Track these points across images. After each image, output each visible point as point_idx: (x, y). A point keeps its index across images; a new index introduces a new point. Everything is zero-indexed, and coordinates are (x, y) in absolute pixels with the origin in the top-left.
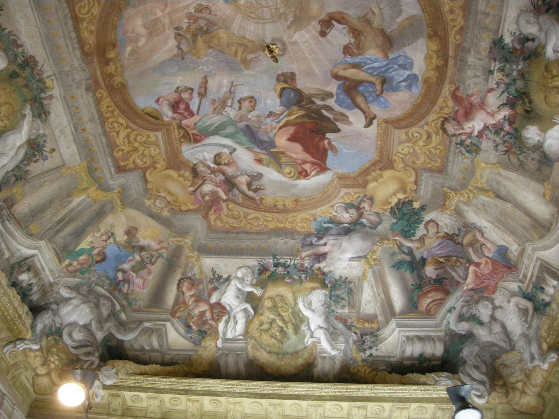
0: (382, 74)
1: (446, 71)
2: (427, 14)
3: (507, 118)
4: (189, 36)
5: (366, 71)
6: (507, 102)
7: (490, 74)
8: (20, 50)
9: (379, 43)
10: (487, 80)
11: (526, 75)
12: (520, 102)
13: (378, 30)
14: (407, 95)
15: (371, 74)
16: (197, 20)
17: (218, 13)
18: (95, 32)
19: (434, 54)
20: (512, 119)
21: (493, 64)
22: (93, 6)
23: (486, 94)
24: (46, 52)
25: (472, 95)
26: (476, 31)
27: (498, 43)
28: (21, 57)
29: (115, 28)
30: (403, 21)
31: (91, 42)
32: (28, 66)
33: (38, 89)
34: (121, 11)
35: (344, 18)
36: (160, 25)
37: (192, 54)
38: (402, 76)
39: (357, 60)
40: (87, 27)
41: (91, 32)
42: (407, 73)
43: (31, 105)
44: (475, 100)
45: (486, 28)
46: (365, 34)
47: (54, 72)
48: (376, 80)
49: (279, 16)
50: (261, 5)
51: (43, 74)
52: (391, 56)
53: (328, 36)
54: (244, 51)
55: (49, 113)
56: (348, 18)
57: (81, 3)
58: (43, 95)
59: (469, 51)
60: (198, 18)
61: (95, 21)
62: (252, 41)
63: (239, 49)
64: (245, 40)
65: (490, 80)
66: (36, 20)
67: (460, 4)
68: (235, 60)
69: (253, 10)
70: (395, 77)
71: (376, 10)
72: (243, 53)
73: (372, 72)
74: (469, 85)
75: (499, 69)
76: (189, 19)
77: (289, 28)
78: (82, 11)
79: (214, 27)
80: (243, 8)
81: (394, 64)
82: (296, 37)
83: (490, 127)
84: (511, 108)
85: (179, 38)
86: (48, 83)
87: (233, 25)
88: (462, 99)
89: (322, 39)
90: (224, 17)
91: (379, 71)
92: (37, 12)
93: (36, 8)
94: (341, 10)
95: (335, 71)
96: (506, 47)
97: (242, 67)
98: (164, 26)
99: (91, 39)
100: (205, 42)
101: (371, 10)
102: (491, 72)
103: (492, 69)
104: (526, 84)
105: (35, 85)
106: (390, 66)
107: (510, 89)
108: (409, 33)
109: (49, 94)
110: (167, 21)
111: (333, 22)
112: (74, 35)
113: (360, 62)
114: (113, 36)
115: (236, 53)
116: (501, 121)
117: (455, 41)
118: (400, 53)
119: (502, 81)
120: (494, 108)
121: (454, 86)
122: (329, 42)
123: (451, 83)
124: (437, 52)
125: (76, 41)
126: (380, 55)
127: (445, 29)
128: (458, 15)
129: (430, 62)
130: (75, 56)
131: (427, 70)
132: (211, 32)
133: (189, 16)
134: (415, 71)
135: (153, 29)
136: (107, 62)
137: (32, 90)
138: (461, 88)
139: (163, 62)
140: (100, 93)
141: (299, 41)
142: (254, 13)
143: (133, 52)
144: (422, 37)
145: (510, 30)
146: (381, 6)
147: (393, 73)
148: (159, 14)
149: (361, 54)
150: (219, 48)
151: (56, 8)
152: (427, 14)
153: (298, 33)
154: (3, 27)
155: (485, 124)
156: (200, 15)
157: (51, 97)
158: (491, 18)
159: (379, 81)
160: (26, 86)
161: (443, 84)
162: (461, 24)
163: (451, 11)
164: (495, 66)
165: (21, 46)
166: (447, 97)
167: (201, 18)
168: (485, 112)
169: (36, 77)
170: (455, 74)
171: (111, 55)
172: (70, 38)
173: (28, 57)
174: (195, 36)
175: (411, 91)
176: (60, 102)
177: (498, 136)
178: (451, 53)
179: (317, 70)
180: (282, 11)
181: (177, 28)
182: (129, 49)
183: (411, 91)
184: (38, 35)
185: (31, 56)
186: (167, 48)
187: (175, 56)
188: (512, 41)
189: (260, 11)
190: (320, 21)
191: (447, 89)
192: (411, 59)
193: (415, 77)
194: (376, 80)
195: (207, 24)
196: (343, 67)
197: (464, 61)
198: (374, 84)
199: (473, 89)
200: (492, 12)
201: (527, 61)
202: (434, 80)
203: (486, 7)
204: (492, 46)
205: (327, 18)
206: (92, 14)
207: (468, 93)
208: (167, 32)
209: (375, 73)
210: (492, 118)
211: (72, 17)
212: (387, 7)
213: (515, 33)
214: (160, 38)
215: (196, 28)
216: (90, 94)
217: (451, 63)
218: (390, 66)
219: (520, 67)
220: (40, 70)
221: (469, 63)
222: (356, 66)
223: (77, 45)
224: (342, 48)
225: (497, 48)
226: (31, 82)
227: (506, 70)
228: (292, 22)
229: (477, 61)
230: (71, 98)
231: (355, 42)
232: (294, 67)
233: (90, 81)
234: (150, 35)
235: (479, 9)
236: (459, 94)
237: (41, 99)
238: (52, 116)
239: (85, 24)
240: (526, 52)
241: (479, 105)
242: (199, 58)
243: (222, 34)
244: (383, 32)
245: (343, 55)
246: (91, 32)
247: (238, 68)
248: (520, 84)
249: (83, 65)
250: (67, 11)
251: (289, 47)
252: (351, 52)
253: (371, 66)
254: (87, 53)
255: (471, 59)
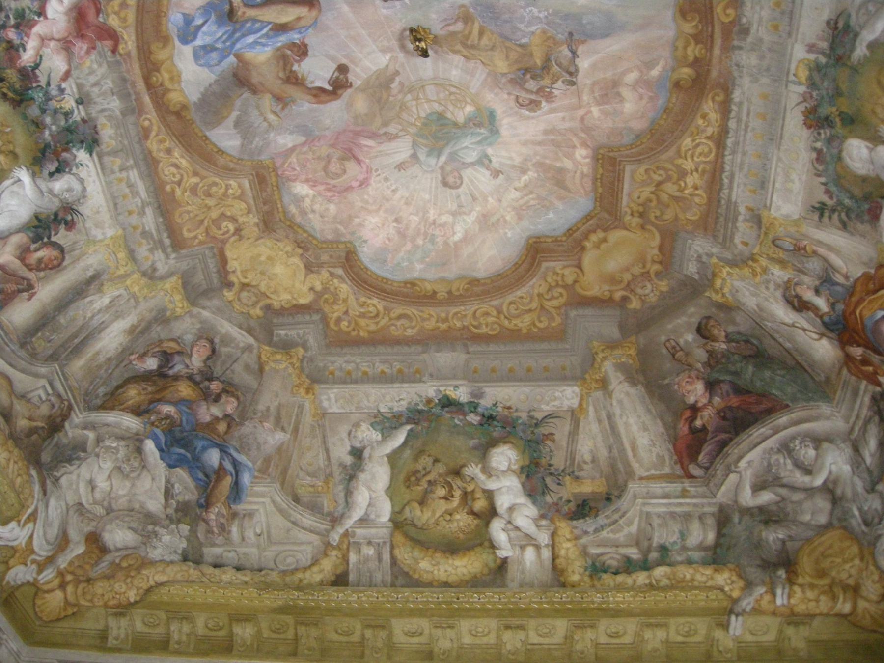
0: (237, 26)
1: (141, 69)
2: (200, 134)
3: (21, 49)
4: (555, 68)
5: (265, 23)
6: (34, 74)
7: (80, 98)
8: (819, 145)
9: (254, 74)
10: (80, 87)
11: (33, 128)
12: (17, 86)
13: (262, 92)
14: (186, 5)
15: (254, 20)
16: (540, 91)
17: (506, 96)
18: (699, 115)
19: (170, 87)
20: (13, 52)
21: (83, 114)
22: (689, 149)
23: (70, 65)
24: (784, 120)
25: (88, 52)
26: (126, 142)
27: (92, 143)
28: (823, 136)
29: (666, 110)
30: (229, 114)
31: (710, 103)
32: (819, 118)
33: (825, 75)
34: (651, 130)
35: (315, 96)
36: (597, 95)
37: (554, 39)
38: (205, 34)
39: (283, 39)
40: (707, 126)
41: (704, 117)
42: (198, 42)
43: (849, 57)
44: (81, 47)
45: (115, 153)
46: (280, 81)
47: (786, 86)
48: (244, 13)
49: (416, 89)
50: (440, 103)
51: (805, 92)
52: (232, 59)
53: (334, 66)
54: (467, 37)
55: (828, 23)
56: (310, 97)
57: (704, 159)
58: (823, 60)
59: (124, 114)
60: (537, 92)
61: (693, 128)
62: (456, 52)
63: (476, 42)
64: (465, 53)
65: (75, 90)
66: (776, 170)
67: (161, 164)
68: (483, 22)
69: (452, 97)
70: (214, 28)
71: (271, 117)
72: (470, 33)
73: (253, 24)
74: (100, 65)
75: (72, 112)
76: (550, 93)
77: (397, 73)
78: (706, 150)
79: (513, 76)
80: (469, 100)
81: (223, 50)
82: (383, 60)
83: (36, 18)
84: (24, 68)
85: (572, 69)
86: (803, 74)
87: (484, 76)
88: (100, 38)
89: (344, 61)
90: (497, 90)
91: (245, 29)
92: (769, 177)
93: (769, 182)
94: (322, 106)
95: (314, 13)
96: (79, 145)
97: (471, 10)
98: (593, 92)
99: (709, 107)
100: (531, 55)
101: (278, 116)
102: (80, 102)
103: (80, 107)
104: (25, 117)
105: (825, 84)
106: (228, 44)
107: (41, 95)
108: (215, 103)
109: (812, 57)
110: (585, 98)
111: (331, 88)
112: (732, 124)
113: (277, 36)
114: (674, 100)
115: (481, 33)
116: (25, 39)
117: (149, 116)
118: (218, 69)
119: (59, 98)
120: (46, 51)
121: (122, 52)
122: (333, 59)
123: (128, 54)
124: (167, 91)
125: (733, 114)
126: (249, 55)
127: (168, 126)
128: (159, 150)
129: (170, 72)
130: (743, 93)
131: (171, 58)
132: (519, 70)
133: (549, 97)
134: (188, 50)
135: (609, 91)
136: (696, 63)
137: (834, 80)
138: (109, 53)
139: (605, 35)
140: (727, 15)
141: (380, 54)
142: (451, 93)
143: (650, 65)
144: (195, 103)
145: (85, 168)
146: (265, 124)
147: (220, 34)
148: (595, 111)
149: (278, 49)
150: (508, 44)
151: (741, 169)
152: (200, 134)
153: (382, 66)
154: (823, 187)
155: (46, 18)
156: (533, 97)
157: (811, 48)
158: (116, 168)
159: (239, 13)
160: (838, 93)
161: (138, 47)
162: (149, 142)
163: (169, 151)
164: (79, 113)
165: (815, 149)
166: (124, 28)
167: (532, 92)
168: (57, 36)
169: (817, 95)
170: (128, 71)
171: (686, 72)
172: (739, 121)
173: (812, 129)
174: (546, 68)
175: (184, 14)
176: (801, 30)
177: (17, 10)
178: (147, 99)
179: (346, 9)
180: (409, 97)
181: (573, 83)
182: (655, 72)
183: (184, 14)
184: (782, 148)
185: (809, 127)
186: (595, 57)
187: (583, 42)
188: (75, 156)
189: (442, 95)
190: (351, 86)
191: (129, 42)
192: (201, 65)
193: (185, 41)
194: (244, 13)
195: (525, 83)
196: (302, 23)
197: (124, 96)
198: (246, 5)
199: (92, 61)
200: (118, 175)
201: (43, 145)
202: (153, 47)
203: (128, 177)
204: (97, 136)
205: (339, 92)
206: (693, 141)
207: (95, 52)
208: (588, 82)
209: (249, 24)
210: (41, 33)
211: (724, 148)
212: (256, 125)
213: (77, 168)
214: (602, 76)
215: (543, 78)
216: (744, 20)
217: (141, 85)
218: (228, 44)
219: (47, 133)
220: (805, 101)
221: (115, 97)
222: (282, 28)
223: (734, 107)
224: (309, 53)
225: (90, 138)
226: (828, 94)
227: (62, 117)
228: (392, 80)
229: (106, 106)
230: (780, 29)
231: (292, 65)
232: (384, 11)
233: (735, 43)
234: (616, 83)
235: (135, 170)
236: (108, 43)
237: (828, 56)
238: (825, 16)
239: (710, 131)
240: (50, 157)
241: (71, 42)
242: (544, 32)
243: (502, 66)
244: (254, 90)
245: (307, 41)
246: (704, 117)
247: (479, 8)
248: (34, 111)
249: (736, 74)
250: (728, 158)
251: (395, 43)
252: (296, 49)
253: (259, 35)
254: (723, 89)
255: (115, 104)
